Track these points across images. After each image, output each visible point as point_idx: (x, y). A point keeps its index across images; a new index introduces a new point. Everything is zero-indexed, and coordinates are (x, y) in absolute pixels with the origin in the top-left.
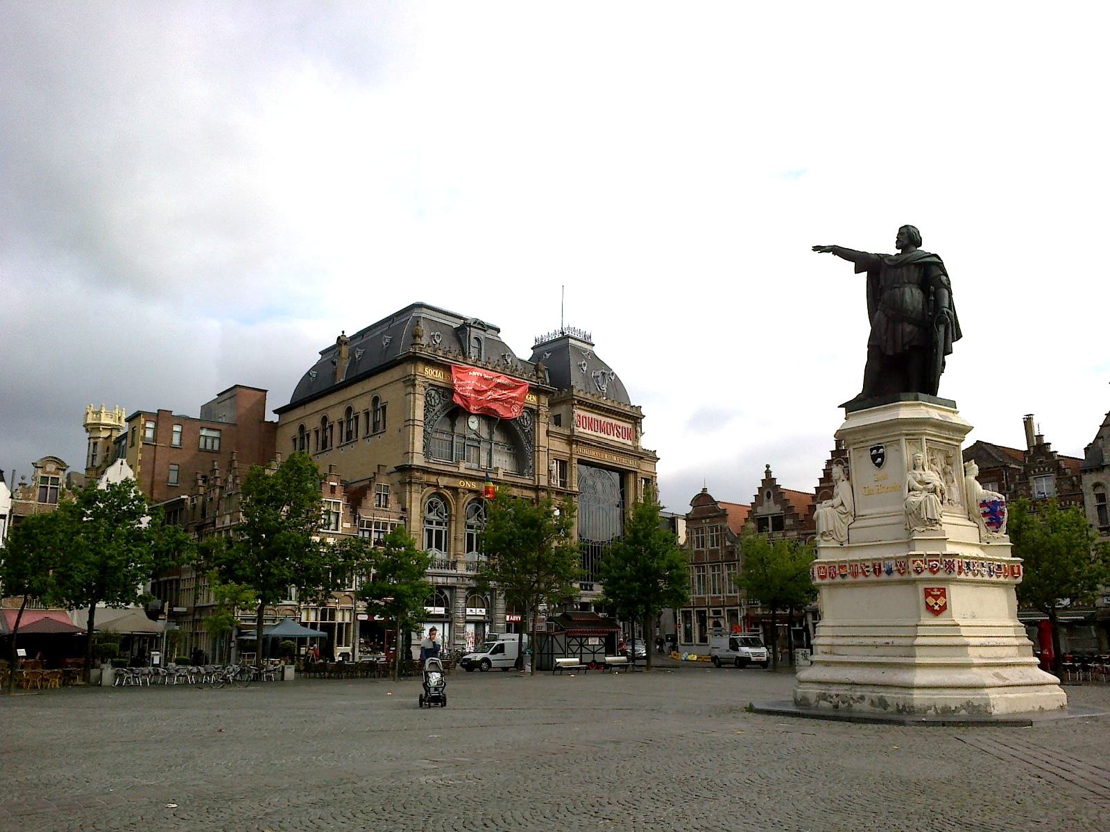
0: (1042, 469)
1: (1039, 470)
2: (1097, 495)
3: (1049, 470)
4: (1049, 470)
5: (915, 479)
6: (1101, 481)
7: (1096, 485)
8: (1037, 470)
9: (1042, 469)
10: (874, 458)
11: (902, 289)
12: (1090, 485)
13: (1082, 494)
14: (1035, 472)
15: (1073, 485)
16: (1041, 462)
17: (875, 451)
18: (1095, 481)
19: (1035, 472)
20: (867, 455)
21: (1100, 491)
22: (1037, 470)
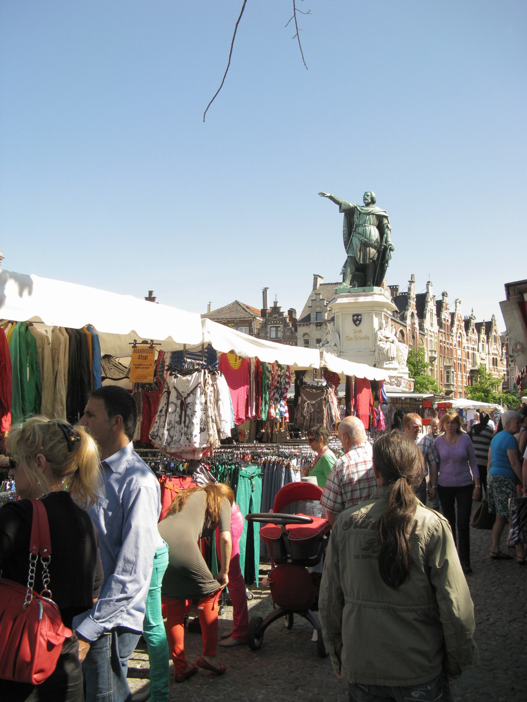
0: (275, 322)
1: (274, 322)
2: (304, 340)
3: (279, 322)
4: (279, 322)
5: (382, 335)
6: (308, 332)
7: (305, 334)
8: (272, 322)
9: (275, 322)
10: (354, 321)
11: (369, 227)
12: (302, 334)
13: (297, 338)
14: (271, 323)
15: (292, 333)
16: (275, 317)
17: (355, 317)
18: (304, 332)
19: (271, 323)
20: (351, 318)
21: (306, 337)
22: (272, 322)
